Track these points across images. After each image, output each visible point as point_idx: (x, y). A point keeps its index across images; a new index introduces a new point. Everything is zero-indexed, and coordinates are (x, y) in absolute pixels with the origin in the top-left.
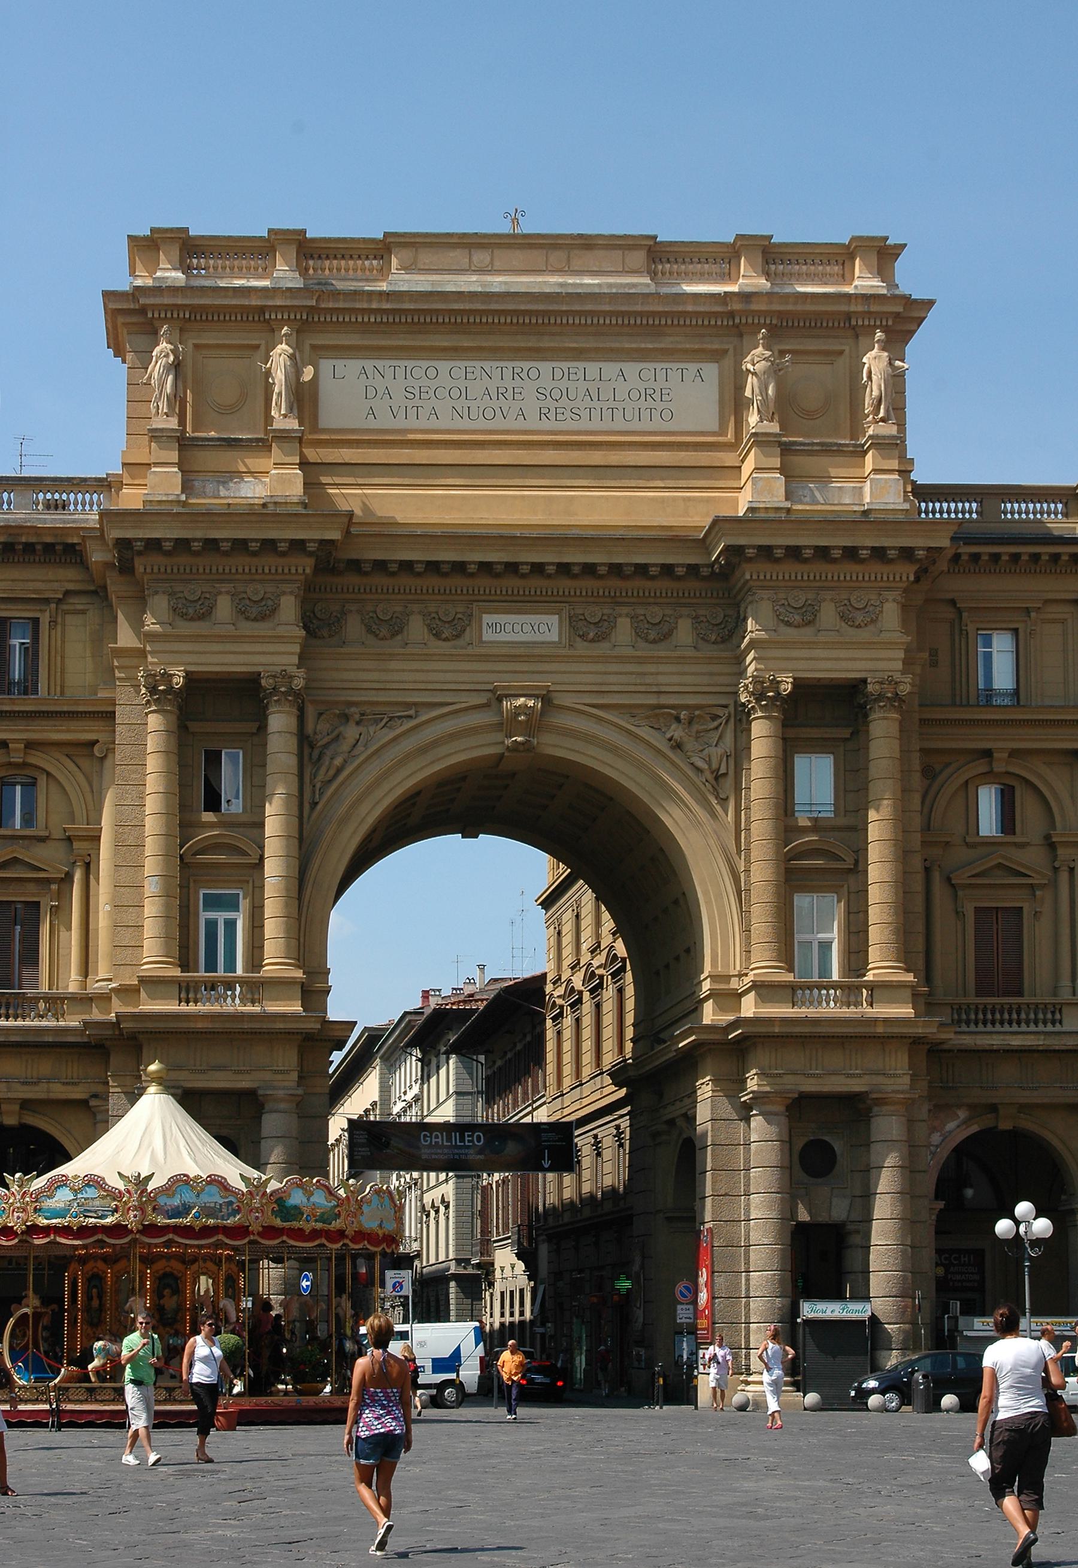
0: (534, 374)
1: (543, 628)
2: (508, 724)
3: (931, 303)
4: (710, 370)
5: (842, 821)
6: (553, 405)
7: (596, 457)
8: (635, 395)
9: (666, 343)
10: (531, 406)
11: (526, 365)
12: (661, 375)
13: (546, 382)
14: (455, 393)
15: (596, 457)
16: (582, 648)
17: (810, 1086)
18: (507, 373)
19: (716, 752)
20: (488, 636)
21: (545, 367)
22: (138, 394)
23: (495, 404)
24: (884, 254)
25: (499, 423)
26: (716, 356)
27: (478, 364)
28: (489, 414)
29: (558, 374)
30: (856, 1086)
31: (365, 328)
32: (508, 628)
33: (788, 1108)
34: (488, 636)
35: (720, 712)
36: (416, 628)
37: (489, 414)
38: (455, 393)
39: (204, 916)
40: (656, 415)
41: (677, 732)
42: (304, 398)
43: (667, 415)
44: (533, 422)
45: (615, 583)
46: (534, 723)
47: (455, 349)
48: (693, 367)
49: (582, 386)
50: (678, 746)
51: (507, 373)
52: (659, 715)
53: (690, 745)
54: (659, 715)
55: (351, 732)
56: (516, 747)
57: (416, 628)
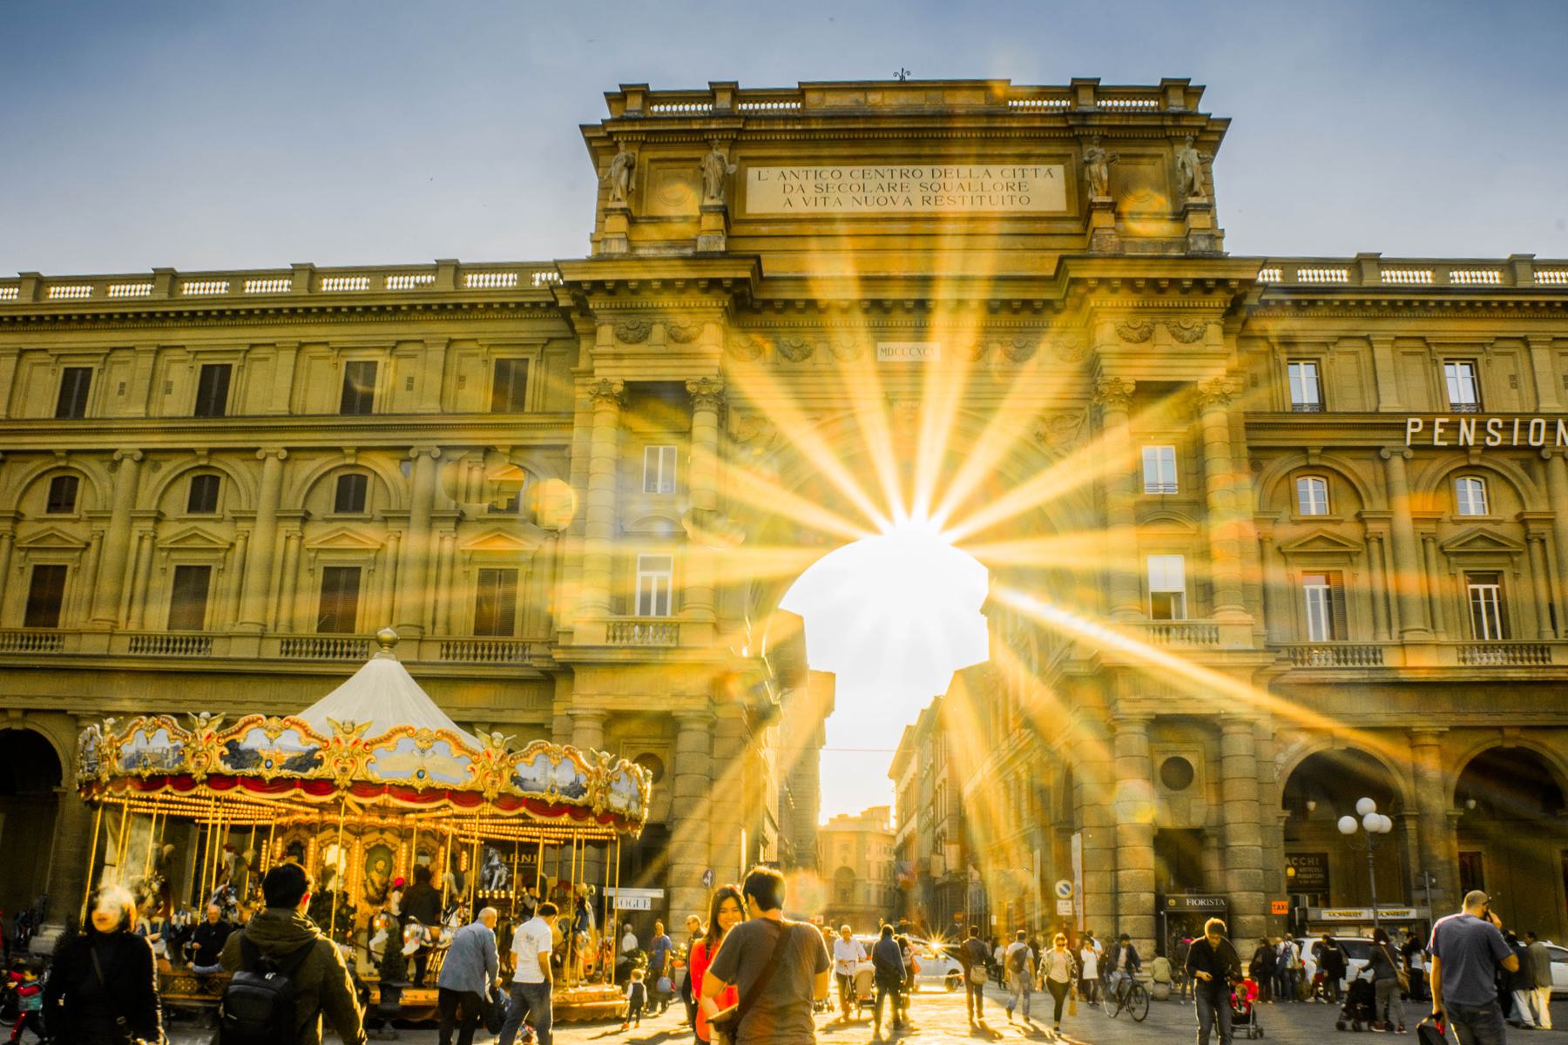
0: (917, 174)
3: (1228, 121)
4: (1059, 170)
5: (1184, 497)
6: (933, 195)
8: (999, 187)
11: (911, 168)
12: (1019, 173)
14: (855, 188)
18: (896, 174)
21: (926, 169)
22: (605, 189)
23: (887, 194)
24: (1193, 93)
25: (890, 208)
26: (1059, 158)
27: (873, 168)
28: (882, 201)
29: (937, 174)
33: (1148, 728)
35: (1078, 413)
37: (882, 201)
38: (855, 188)
40: (1016, 200)
43: (1024, 200)
47: (854, 157)
48: (1043, 168)
49: (956, 181)
51: (896, 174)
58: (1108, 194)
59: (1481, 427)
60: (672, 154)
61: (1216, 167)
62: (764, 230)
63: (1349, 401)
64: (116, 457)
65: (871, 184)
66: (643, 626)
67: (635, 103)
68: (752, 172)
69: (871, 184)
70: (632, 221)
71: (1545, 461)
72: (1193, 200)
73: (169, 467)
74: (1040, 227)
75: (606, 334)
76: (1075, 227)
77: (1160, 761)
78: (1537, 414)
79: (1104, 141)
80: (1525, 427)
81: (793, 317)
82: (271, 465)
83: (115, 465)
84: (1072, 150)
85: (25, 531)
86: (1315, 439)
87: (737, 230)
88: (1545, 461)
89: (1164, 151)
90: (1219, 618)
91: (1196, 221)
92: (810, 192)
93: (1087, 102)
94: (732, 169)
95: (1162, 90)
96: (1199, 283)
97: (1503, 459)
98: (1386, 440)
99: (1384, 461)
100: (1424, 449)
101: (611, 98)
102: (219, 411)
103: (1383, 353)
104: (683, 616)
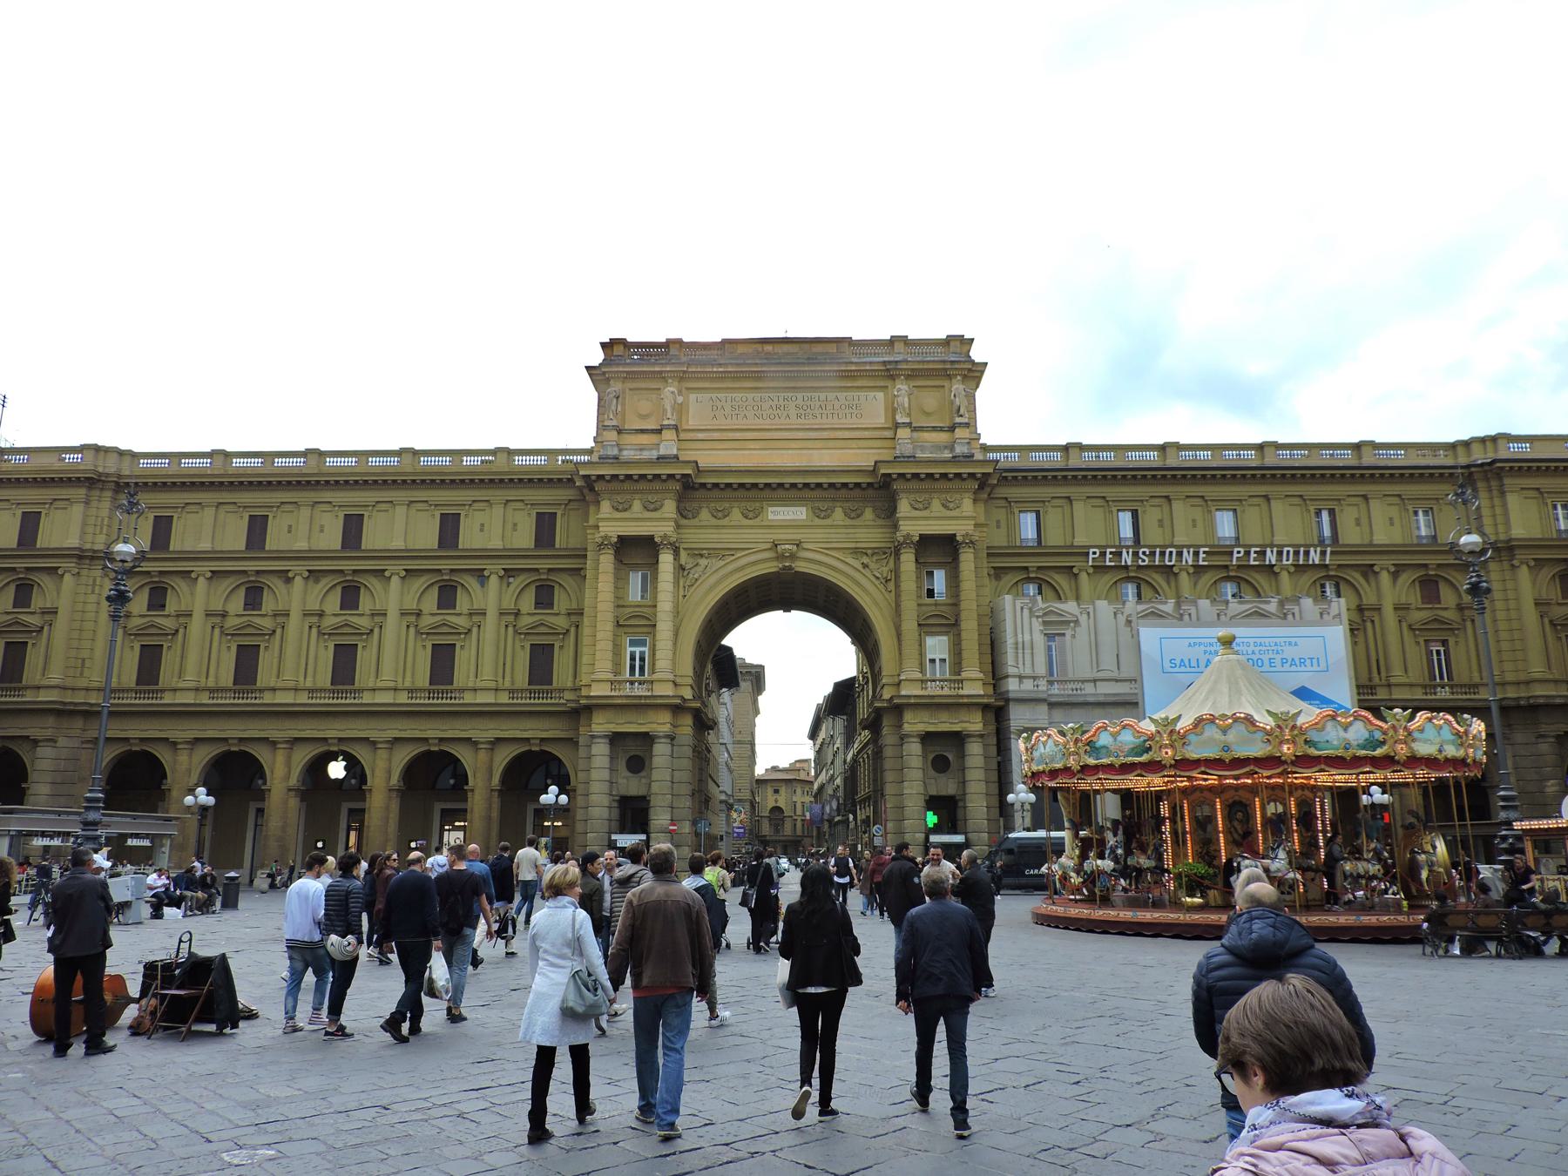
1: (799, 513)
2: (781, 557)
4: (880, 395)
7: (825, 434)
9: (859, 383)
10: (793, 412)
13: (799, 401)
15: (825, 434)
16: (818, 521)
17: (931, 729)
19: (885, 569)
20: (771, 517)
21: (800, 395)
30: (956, 728)
31: (712, 379)
32: (780, 513)
34: (771, 517)
36: (736, 515)
39: (629, 649)
41: (865, 560)
42: (680, 409)
44: (794, 422)
45: (832, 491)
46: (793, 557)
50: (865, 566)
52: (857, 552)
53: (872, 565)
54: (857, 552)
55: (703, 562)
56: (785, 568)
57: (736, 515)
58: (909, 415)
59: (1136, 554)
60: (643, 385)
61: (980, 394)
62: (701, 436)
63: (1054, 538)
64: (290, 575)
65: (766, 406)
66: (632, 683)
67: (618, 350)
68: (693, 397)
69: (766, 406)
70: (620, 432)
71: (1176, 575)
72: (958, 420)
73: (326, 582)
74: (867, 434)
75: (605, 506)
76: (889, 434)
77: (931, 757)
78: (1172, 546)
79: (908, 377)
80: (1163, 554)
81: (716, 493)
82: (395, 579)
83: (289, 581)
84: (889, 383)
85: (231, 622)
86: (1032, 563)
87: (683, 436)
88: (1176, 575)
89: (946, 383)
90: (964, 675)
91: (959, 433)
92: (728, 410)
93: (899, 354)
94: (680, 399)
95: (949, 340)
96: (958, 475)
97: (1149, 572)
98: (1076, 563)
99: (1076, 575)
100: (1100, 569)
101: (603, 345)
102: (358, 546)
103: (1078, 506)
104: (655, 677)
